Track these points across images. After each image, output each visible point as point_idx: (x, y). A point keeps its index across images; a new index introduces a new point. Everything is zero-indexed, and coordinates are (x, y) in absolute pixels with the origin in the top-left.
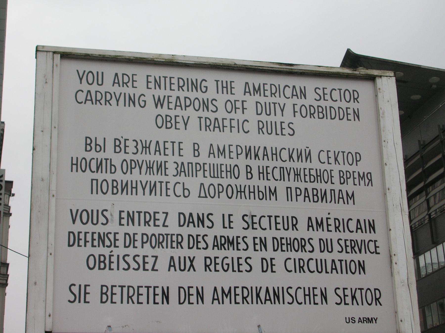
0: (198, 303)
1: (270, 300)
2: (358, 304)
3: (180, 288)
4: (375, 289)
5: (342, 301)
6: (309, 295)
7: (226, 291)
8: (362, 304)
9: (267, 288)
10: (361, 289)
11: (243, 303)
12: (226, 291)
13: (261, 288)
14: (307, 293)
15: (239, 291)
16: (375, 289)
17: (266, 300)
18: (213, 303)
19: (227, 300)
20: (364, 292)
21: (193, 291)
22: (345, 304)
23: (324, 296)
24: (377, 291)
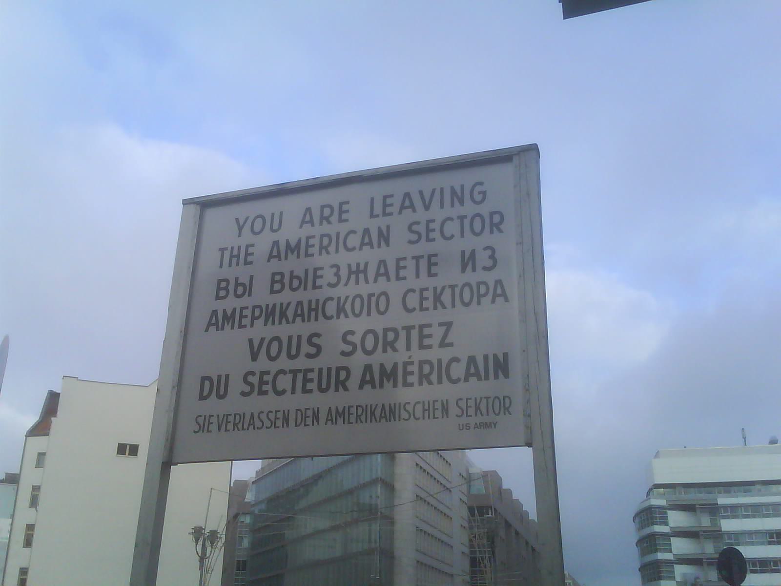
0: (313, 425)
1: (385, 417)
2: (482, 415)
3: (297, 410)
4: (505, 397)
5: (464, 413)
6: (428, 410)
7: (341, 410)
8: (488, 415)
9: (383, 406)
10: (487, 398)
11: (357, 422)
12: (341, 410)
13: (377, 405)
14: (426, 407)
15: (353, 410)
16: (505, 397)
17: (381, 417)
18: (326, 424)
19: (340, 421)
20: (491, 401)
21: (310, 413)
22: (467, 416)
23: (445, 410)
24: (507, 400)
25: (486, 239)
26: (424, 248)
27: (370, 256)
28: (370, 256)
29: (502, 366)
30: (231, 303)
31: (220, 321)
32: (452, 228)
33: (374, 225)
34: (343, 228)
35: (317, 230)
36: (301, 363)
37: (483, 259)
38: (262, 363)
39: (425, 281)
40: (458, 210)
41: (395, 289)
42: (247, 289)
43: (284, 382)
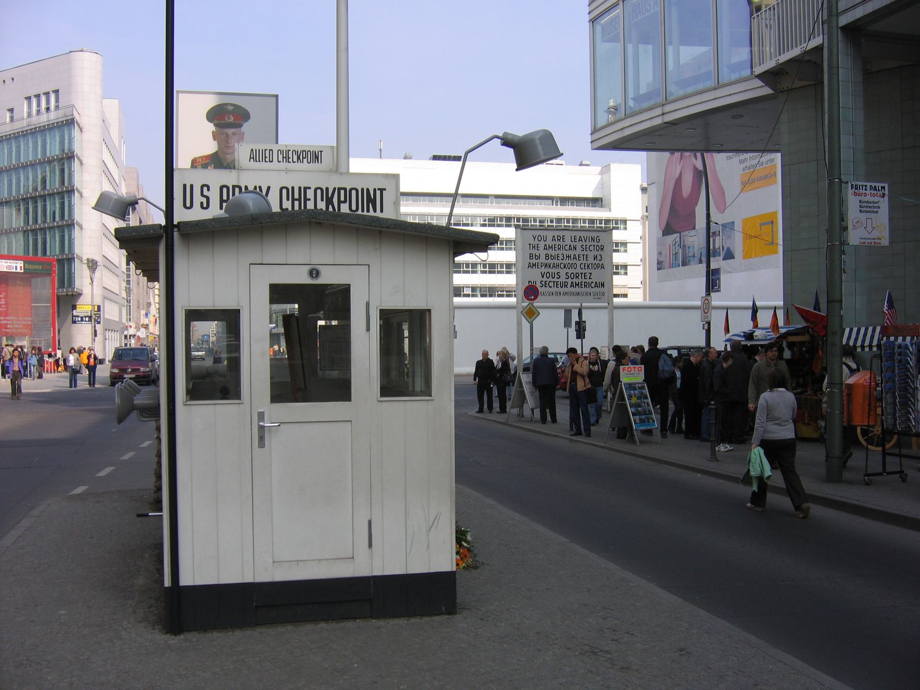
25: (600, 252)
26: (585, 253)
27: (572, 253)
28: (572, 253)
29: (603, 285)
30: (534, 261)
31: (532, 266)
32: (592, 248)
33: (572, 244)
34: (564, 244)
35: (557, 243)
36: (555, 280)
37: (599, 258)
38: (545, 279)
39: (585, 261)
40: (593, 243)
41: (578, 263)
42: (539, 258)
43: (551, 284)
